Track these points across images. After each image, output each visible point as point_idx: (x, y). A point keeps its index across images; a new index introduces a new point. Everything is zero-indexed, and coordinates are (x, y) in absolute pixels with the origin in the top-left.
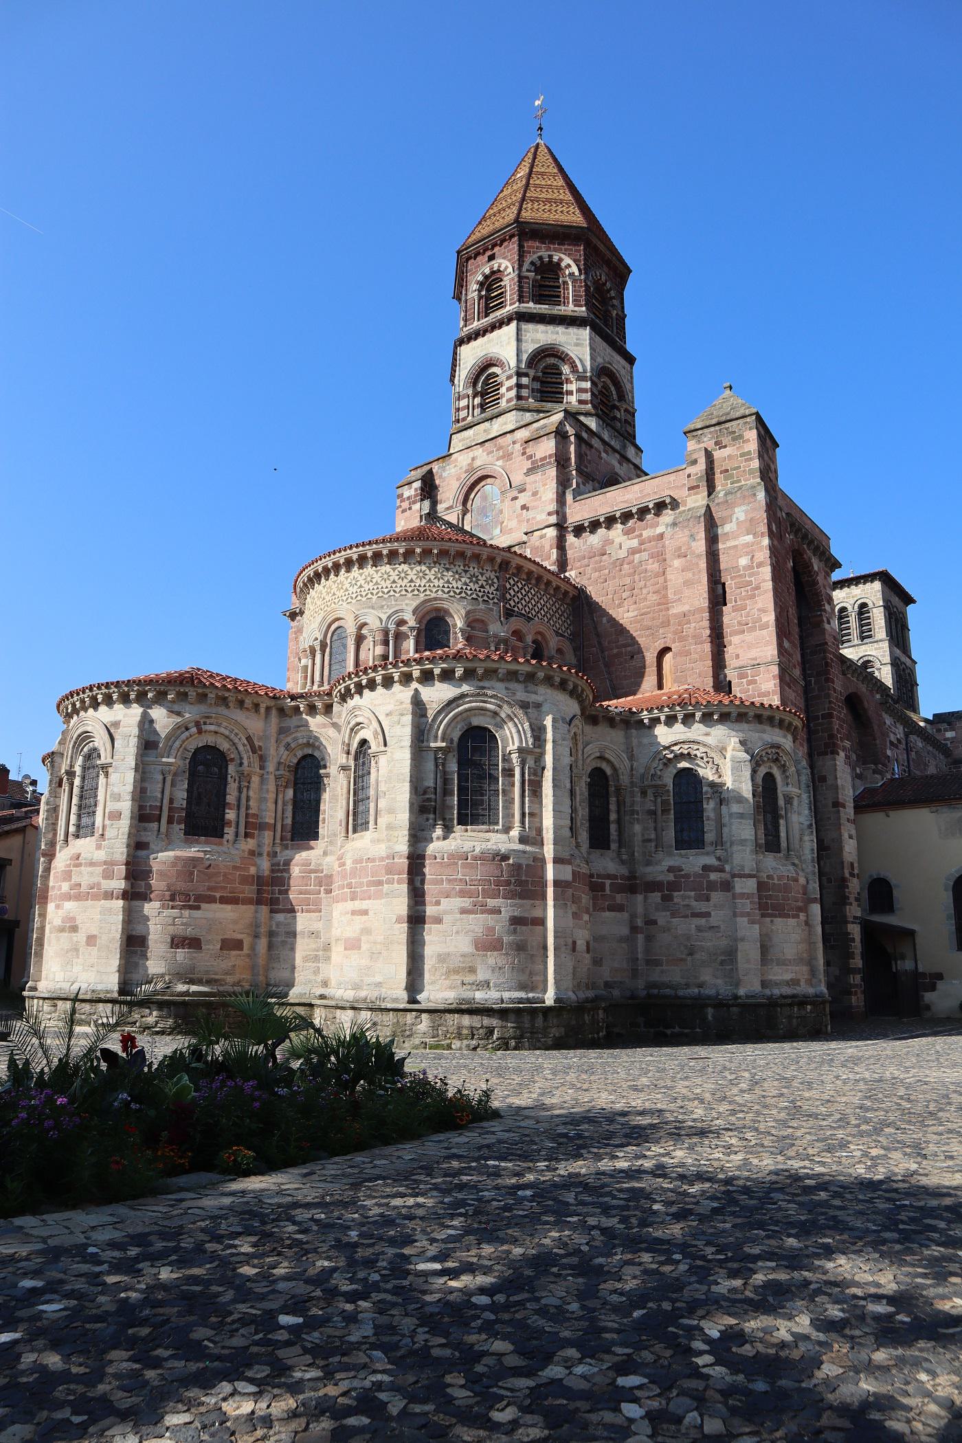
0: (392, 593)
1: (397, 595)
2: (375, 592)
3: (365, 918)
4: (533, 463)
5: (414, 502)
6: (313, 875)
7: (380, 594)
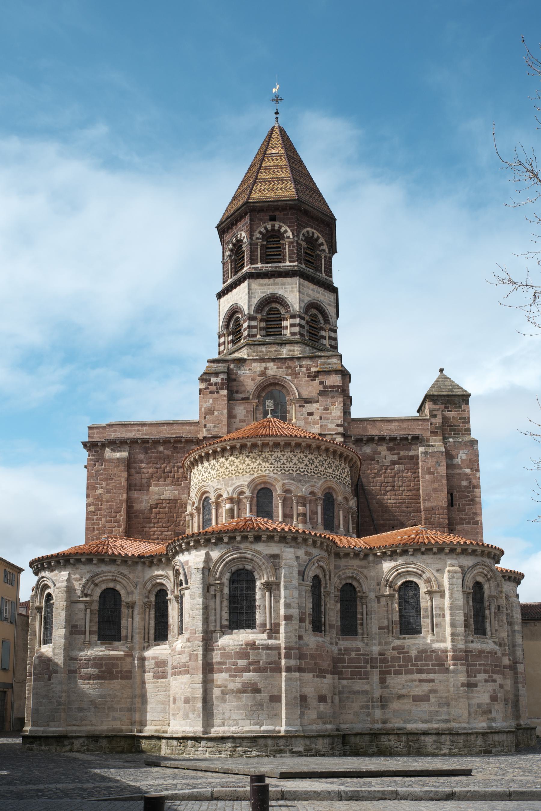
0: (306, 473)
1: (309, 475)
2: (295, 469)
3: (431, 684)
4: (324, 387)
5: (222, 389)
6: (362, 657)
7: (298, 472)
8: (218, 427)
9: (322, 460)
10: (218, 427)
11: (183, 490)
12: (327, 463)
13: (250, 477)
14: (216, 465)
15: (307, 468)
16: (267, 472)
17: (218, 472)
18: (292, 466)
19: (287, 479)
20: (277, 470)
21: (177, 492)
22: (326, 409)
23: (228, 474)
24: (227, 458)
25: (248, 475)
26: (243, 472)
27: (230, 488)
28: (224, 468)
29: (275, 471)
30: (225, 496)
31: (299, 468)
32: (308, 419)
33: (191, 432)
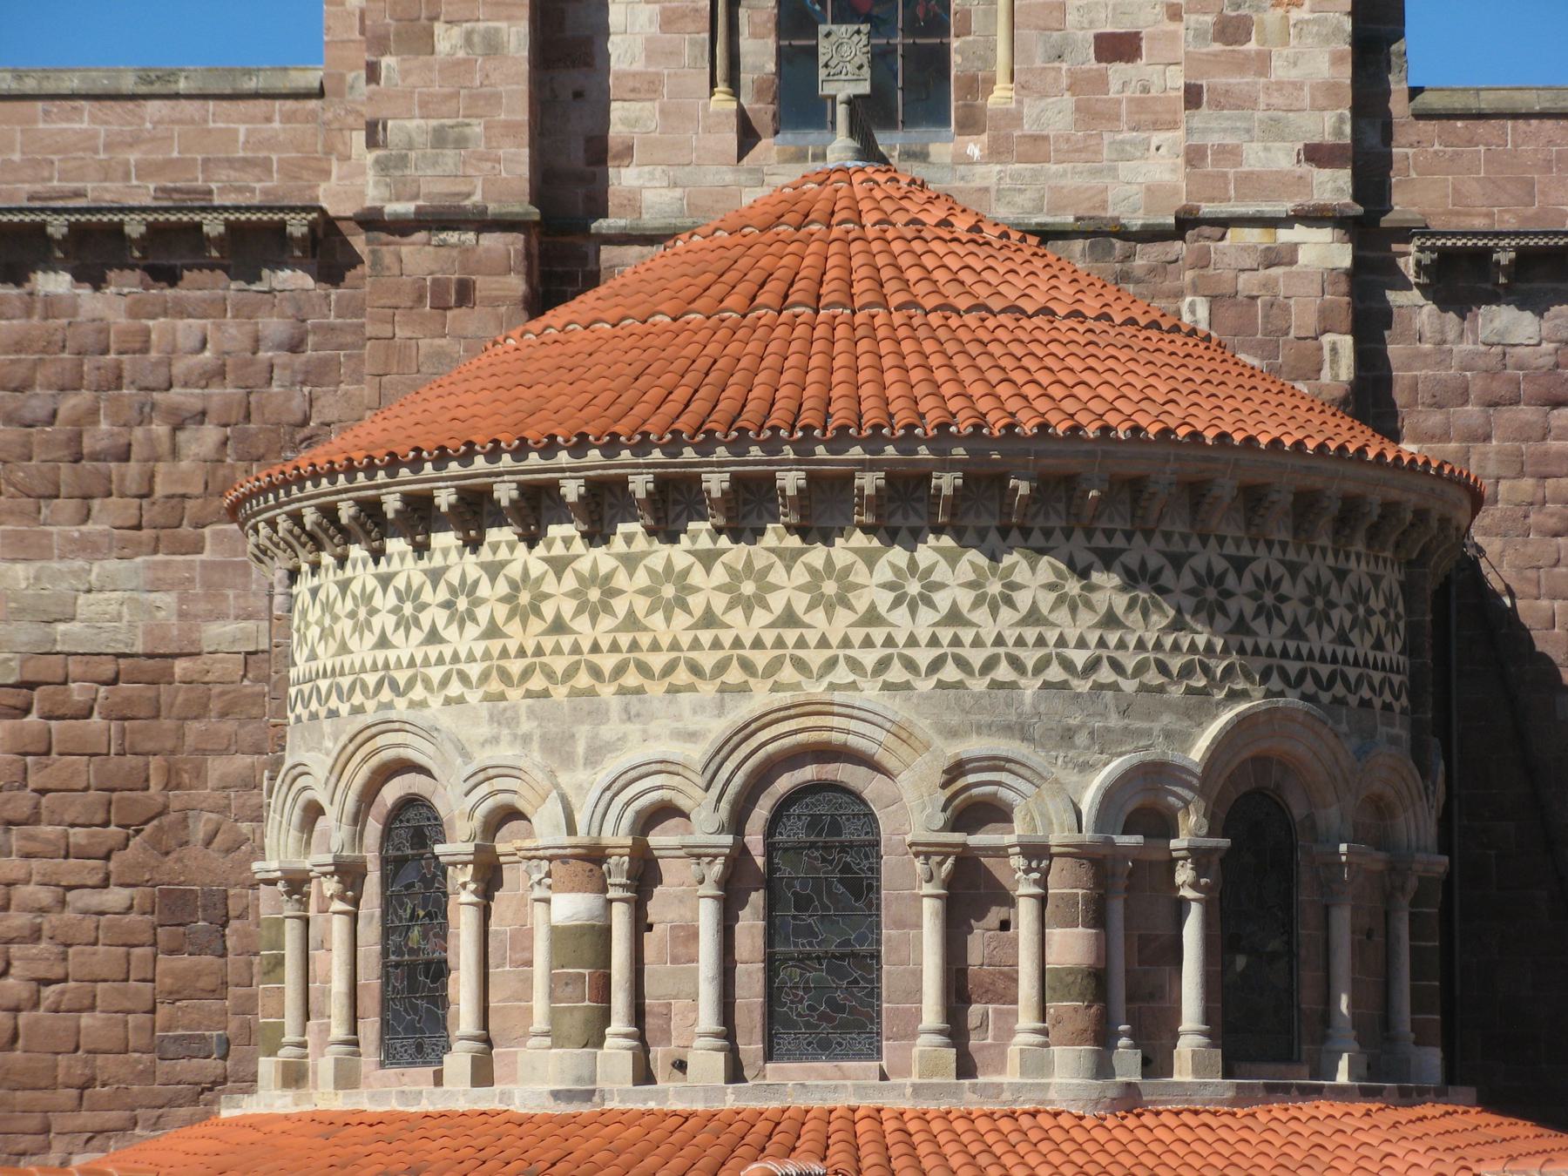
0: (1105, 674)
1: (1129, 686)
2: (1030, 657)
7: (1055, 673)
8: (461, 142)
9: (1220, 565)
10: (461, 142)
11: (213, 591)
12: (1248, 584)
13: (721, 709)
14: (484, 590)
15: (1113, 638)
16: (842, 674)
17: (496, 646)
18: (1010, 636)
19: (979, 729)
20: (910, 665)
21: (167, 600)
22: (1232, 30)
23: (571, 672)
24: (558, 550)
25: (708, 689)
26: (670, 669)
27: (582, 775)
28: (536, 625)
29: (896, 673)
30: (546, 829)
31: (1061, 642)
32: (1102, 82)
33: (266, 165)
